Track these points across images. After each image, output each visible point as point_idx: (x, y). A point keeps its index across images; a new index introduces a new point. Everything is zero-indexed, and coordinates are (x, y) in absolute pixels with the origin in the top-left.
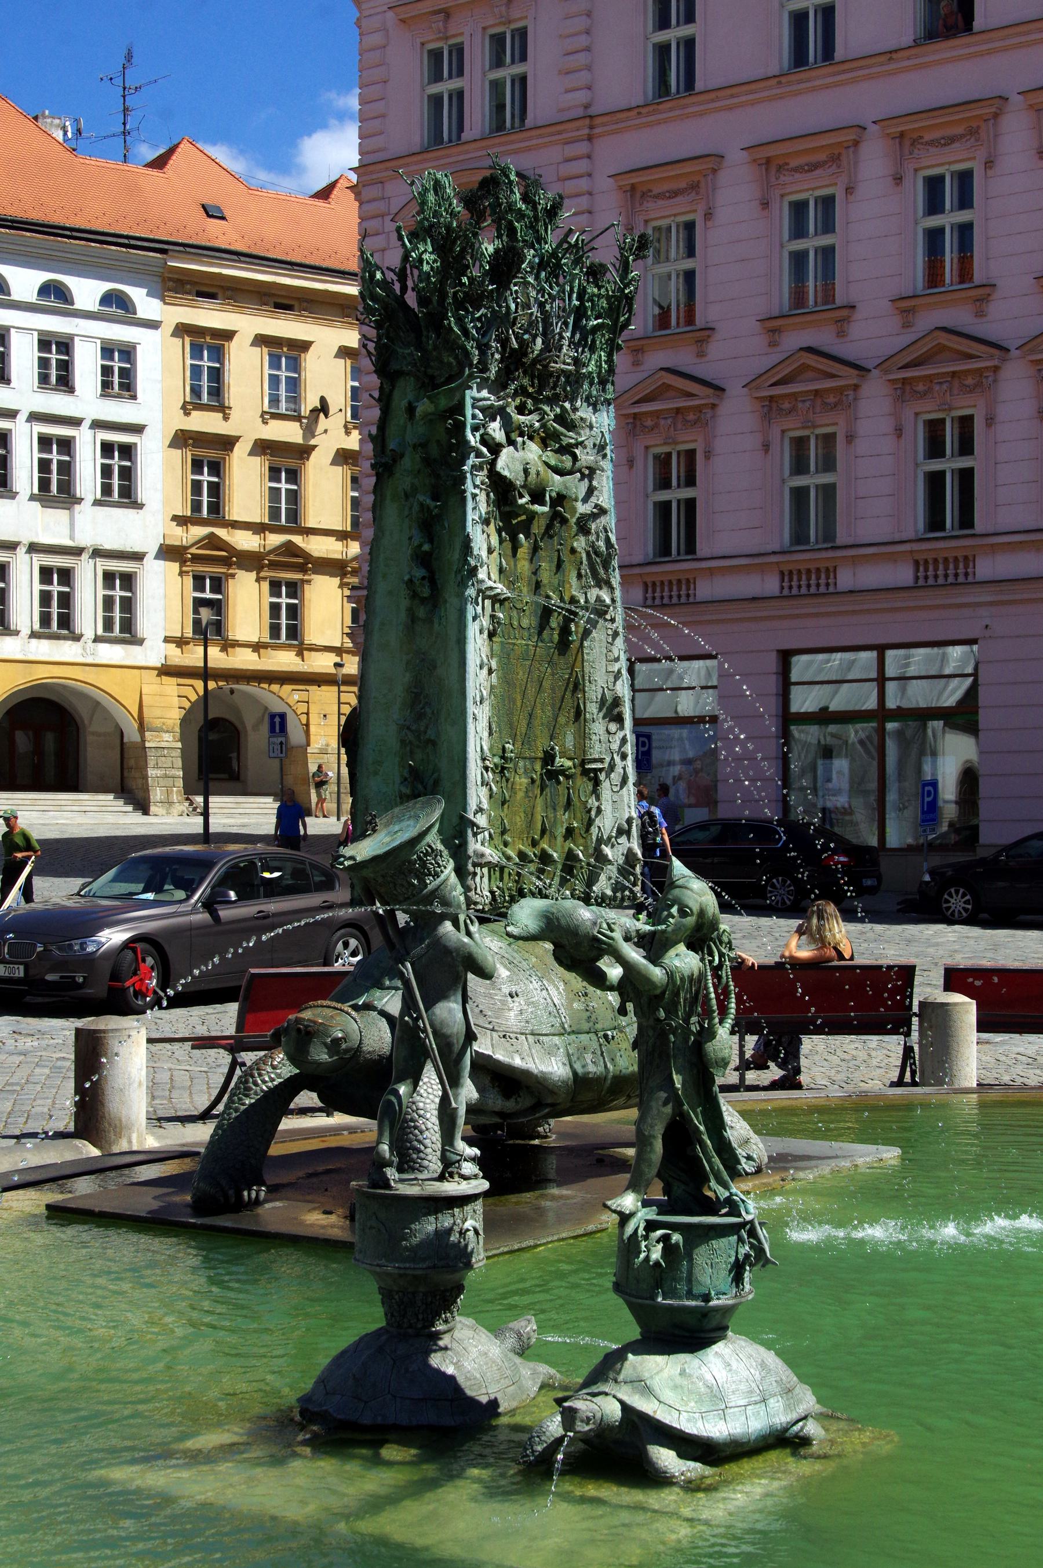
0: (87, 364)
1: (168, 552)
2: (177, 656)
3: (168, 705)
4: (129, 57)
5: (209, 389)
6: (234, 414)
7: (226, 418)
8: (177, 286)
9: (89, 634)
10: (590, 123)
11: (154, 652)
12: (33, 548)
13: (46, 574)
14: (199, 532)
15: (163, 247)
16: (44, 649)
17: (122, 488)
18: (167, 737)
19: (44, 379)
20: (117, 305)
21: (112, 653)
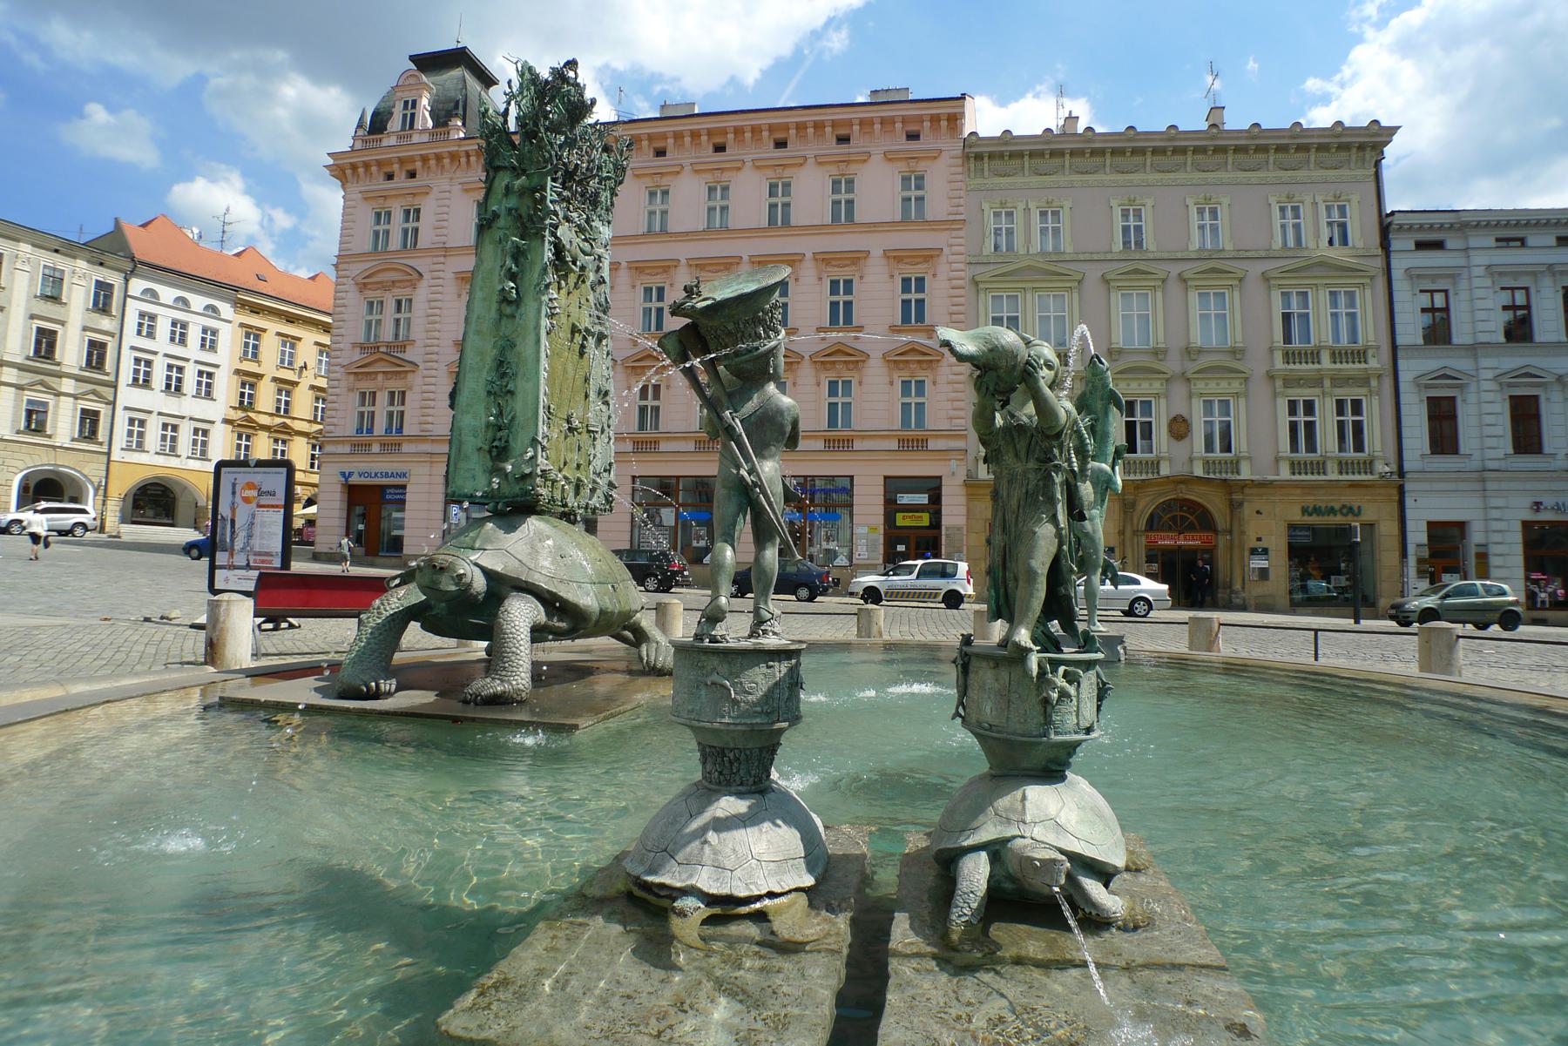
5: (252, 351)
8: (241, 305)
9: (184, 455)
10: (446, 251)
12: (160, 414)
15: (236, 289)
16: (161, 460)
17: (206, 391)
19: (172, 339)
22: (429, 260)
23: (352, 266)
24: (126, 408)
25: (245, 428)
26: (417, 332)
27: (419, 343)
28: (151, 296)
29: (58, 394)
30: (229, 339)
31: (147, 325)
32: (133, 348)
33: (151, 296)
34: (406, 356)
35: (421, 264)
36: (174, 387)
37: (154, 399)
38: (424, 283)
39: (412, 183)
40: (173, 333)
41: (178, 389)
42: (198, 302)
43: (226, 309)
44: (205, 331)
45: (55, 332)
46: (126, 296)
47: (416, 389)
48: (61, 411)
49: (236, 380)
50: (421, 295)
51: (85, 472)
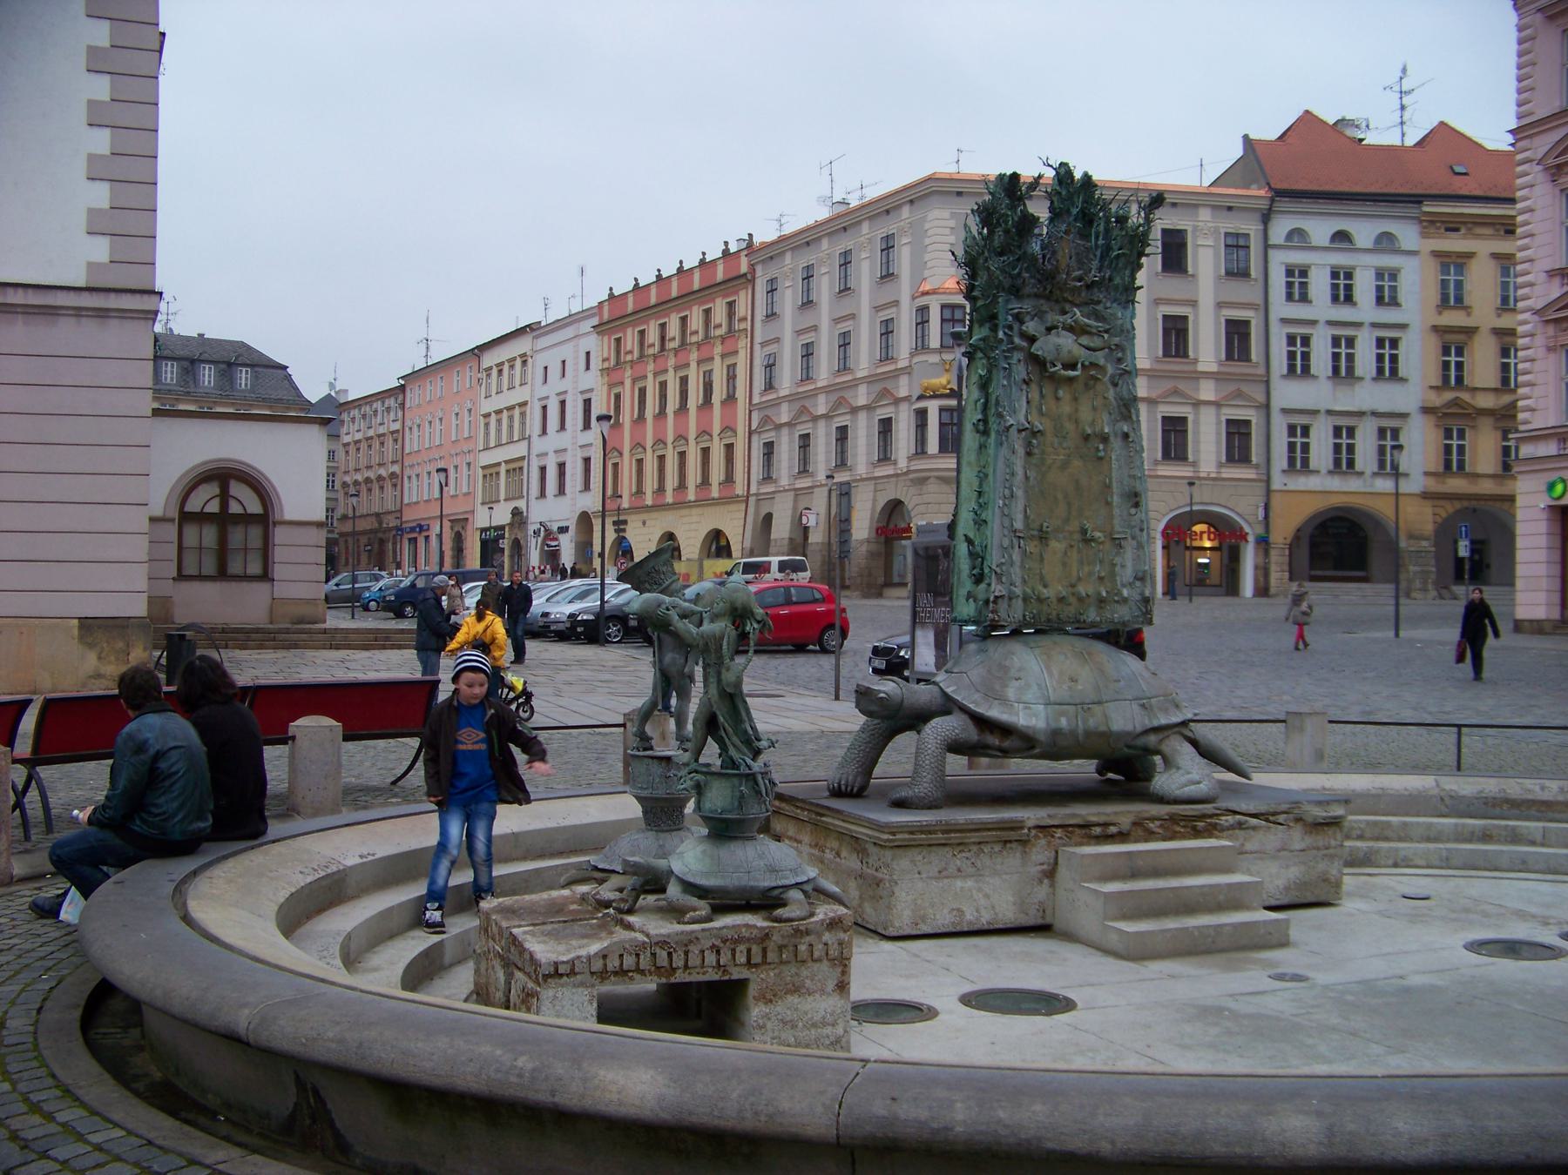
0: (1364, 287)
1: (1426, 410)
2: (1432, 485)
3: (1420, 519)
4: (1404, 70)
5: (1451, 297)
6: (1476, 312)
7: (1469, 314)
8: (1431, 225)
11: (1414, 484)
12: (1329, 412)
13: (1337, 431)
14: (1449, 396)
15: (1417, 199)
16: (1335, 483)
17: (1388, 369)
18: (1424, 543)
19: (1335, 299)
20: (1386, 242)
23: (1537, 141)
24: (1285, 411)
25: (1453, 419)
28: (1297, 237)
29: (1197, 404)
30: (1417, 284)
31: (1298, 286)
32: (1284, 321)
33: (1297, 237)
36: (1343, 371)
40: (1335, 287)
41: (1350, 369)
42: (1364, 231)
43: (1407, 234)
44: (1379, 275)
45: (1185, 318)
46: (1267, 246)
48: (1203, 428)
49: (1433, 343)
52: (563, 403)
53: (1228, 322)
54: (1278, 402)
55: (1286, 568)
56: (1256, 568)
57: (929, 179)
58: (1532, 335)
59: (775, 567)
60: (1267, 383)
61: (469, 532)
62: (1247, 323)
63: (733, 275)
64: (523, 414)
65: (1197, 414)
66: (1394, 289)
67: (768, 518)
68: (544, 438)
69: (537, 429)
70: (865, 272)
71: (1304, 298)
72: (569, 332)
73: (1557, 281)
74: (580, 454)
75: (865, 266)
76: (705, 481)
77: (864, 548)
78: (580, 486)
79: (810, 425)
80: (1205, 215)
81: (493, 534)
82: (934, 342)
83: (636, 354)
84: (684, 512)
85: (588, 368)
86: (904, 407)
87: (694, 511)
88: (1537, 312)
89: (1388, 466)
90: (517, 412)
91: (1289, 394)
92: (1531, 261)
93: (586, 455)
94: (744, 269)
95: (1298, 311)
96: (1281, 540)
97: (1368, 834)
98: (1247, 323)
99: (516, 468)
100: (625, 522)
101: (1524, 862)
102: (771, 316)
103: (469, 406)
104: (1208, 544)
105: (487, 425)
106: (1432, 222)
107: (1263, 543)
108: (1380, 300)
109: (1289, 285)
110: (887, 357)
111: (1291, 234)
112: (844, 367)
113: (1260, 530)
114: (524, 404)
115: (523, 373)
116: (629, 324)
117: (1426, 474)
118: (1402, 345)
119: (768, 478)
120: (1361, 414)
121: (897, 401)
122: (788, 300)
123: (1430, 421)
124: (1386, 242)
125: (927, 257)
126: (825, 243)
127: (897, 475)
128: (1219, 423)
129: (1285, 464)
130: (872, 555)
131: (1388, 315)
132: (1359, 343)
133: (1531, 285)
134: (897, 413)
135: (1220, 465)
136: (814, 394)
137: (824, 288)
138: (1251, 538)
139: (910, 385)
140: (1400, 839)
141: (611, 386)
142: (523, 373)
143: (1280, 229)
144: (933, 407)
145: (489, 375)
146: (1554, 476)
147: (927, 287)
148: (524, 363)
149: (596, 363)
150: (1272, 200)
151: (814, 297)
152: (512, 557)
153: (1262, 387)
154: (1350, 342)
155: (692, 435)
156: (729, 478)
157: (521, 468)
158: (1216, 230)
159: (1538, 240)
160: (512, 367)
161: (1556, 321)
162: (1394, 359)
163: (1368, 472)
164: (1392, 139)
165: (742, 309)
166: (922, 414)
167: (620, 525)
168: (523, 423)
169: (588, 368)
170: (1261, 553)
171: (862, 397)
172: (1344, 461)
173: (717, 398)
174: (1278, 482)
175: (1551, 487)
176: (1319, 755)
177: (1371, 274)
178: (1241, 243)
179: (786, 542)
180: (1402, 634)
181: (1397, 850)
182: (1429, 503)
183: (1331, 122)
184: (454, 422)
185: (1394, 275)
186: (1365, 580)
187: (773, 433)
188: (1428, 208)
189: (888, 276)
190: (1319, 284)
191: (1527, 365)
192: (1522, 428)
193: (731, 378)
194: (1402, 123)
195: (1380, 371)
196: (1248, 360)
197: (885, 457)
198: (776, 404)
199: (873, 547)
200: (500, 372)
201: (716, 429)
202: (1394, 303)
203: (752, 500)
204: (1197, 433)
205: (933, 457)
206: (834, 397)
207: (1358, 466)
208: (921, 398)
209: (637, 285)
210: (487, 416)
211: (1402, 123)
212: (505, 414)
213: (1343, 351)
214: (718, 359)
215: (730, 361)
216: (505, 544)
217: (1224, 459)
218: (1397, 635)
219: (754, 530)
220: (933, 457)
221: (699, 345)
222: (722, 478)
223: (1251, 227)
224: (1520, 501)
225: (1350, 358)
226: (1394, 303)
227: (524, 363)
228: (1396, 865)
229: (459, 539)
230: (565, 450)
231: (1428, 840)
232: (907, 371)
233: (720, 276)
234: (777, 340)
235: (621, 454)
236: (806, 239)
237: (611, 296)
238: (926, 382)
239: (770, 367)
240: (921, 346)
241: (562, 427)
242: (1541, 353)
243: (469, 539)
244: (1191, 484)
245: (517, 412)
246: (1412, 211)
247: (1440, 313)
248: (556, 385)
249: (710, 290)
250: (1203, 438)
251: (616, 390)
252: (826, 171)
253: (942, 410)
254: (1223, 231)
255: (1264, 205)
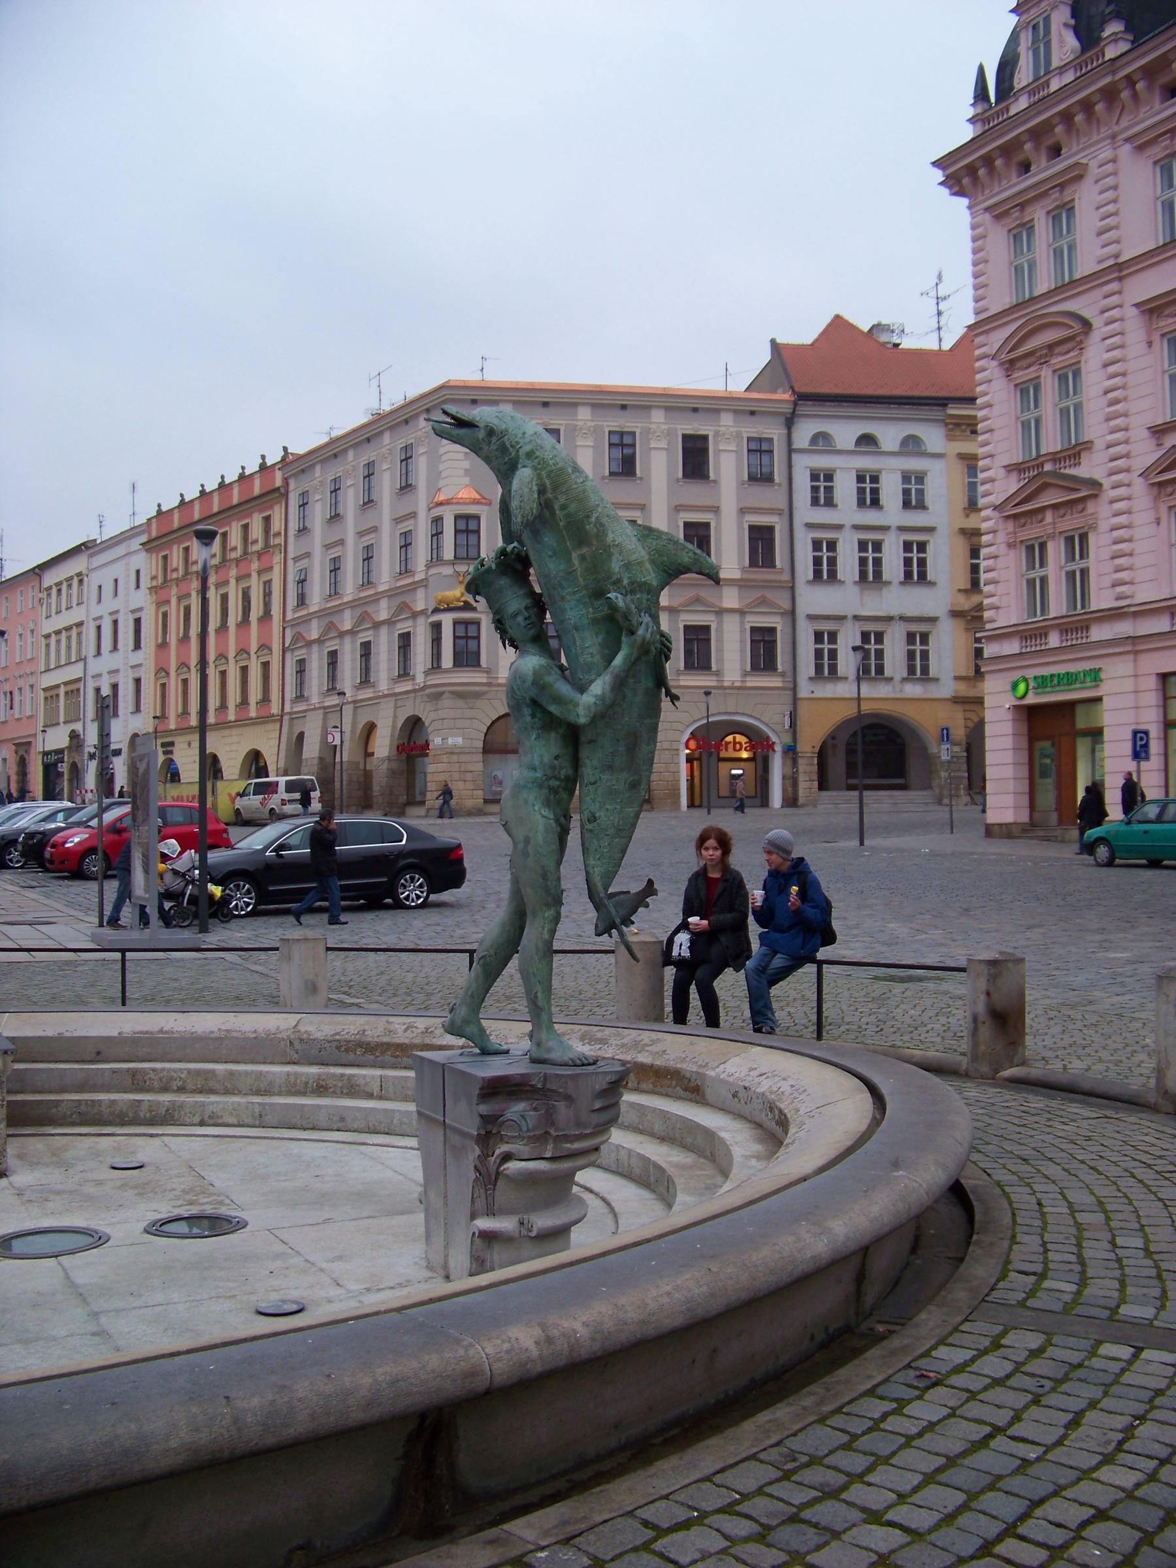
0: (891, 490)
1: (955, 614)
4: (940, 277)
10: (1120, 270)
12: (856, 618)
15: (942, 402)
17: (916, 574)
19: (861, 503)
20: (911, 445)
21: (913, 690)
22: (1097, 294)
24: (811, 617)
26: (1094, 428)
27: (1099, 444)
28: (821, 440)
29: (720, 612)
31: (823, 488)
32: (809, 526)
33: (821, 440)
34: (1083, 471)
35: (1085, 305)
36: (871, 575)
37: (841, 599)
38: (1095, 336)
39: (1060, 165)
40: (861, 491)
41: (878, 574)
42: (890, 434)
43: (933, 437)
44: (906, 478)
45: (707, 525)
46: (790, 451)
47: (1103, 526)
48: (726, 636)
50: (1094, 355)
51: (766, 720)
52: (115, 622)
53: (752, 528)
54: (803, 609)
55: (815, 777)
56: (784, 778)
57: (442, 387)
58: (995, 532)
59: (282, 787)
60: (793, 589)
61: (32, 755)
62: (770, 529)
63: (264, 492)
64: (79, 634)
65: (720, 623)
66: (920, 492)
67: (301, 736)
68: (99, 658)
69: (92, 650)
70: (386, 483)
71: (830, 503)
72: (120, 550)
73: (1014, 476)
74: (131, 675)
75: (387, 477)
76: (244, 702)
77: (385, 766)
78: (131, 707)
79: (337, 641)
80: (727, 420)
81: (54, 757)
82: (448, 553)
83: (181, 572)
84: (226, 732)
85: (138, 587)
86: (421, 621)
87: (234, 731)
88: (996, 508)
89: (918, 667)
90: (74, 632)
91: (815, 600)
92: (991, 456)
93: (137, 676)
94: (278, 482)
95: (823, 516)
96: (809, 749)
97: (190, 1086)
98: (770, 529)
99: (73, 689)
100: (172, 744)
101: (342, 1119)
102: (303, 530)
103: (32, 626)
104: (745, 755)
105: (48, 646)
106: (957, 425)
107: (791, 751)
108: (906, 504)
109: (815, 489)
110: (406, 570)
111: (815, 439)
112: (368, 583)
113: (788, 739)
114: (80, 624)
115: (80, 592)
116: (172, 542)
117: (956, 678)
118: (930, 548)
119: (300, 697)
120: (890, 619)
121: (415, 615)
122: (318, 513)
123: (960, 624)
124: (911, 445)
125: (442, 467)
126: (351, 454)
127: (414, 691)
128: (743, 631)
129: (812, 673)
130: (393, 773)
131: (915, 519)
132: (885, 548)
133: (993, 480)
134: (415, 627)
135: (745, 674)
136: (339, 610)
137: (351, 499)
138: (778, 748)
139: (426, 598)
140: (227, 1092)
141: (159, 605)
142: (80, 592)
143: (804, 432)
144: (447, 620)
145: (49, 595)
146: (1017, 675)
147: (442, 497)
148: (81, 582)
149: (145, 582)
150: (795, 404)
151: (341, 510)
152: (70, 781)
153: (786, 595)
154: (878, 546)
155: (231, 654)
156: (266, 699)
157: (78, 690)
158: (738, 435)
159: (997, 435)
160: (70, 586)
161: (1015, 517)
162: (922, 563)
163: (898, 678)
164: (931, 344)
165: (277, 525)
166: (437, 627)
167: (168, 747)
168: (79, 643)
169: (138, 587)
170: (789, 762)
171: (383, 612)
172: (871, 667)
173: (254, 616)
174: (803, 693)
175: (1015, 686)
176: (312, 988)
177: (898, 478)
178: (765, 447)
179: (316, 762)
180: (866, 843)
181: (203, 1105)
182: (959, 708)
183: (865, 328)
184: (18, 643)
185: (920, 479)
186: (904, 787)
187: (304, 651)
188: (952, 410)
189: (407, 487)
190: (845, 488)
191: (991, 562)
192: (988, 626)
193: (267, 595)
194: (939, 329)
195: (908, 575)
196: (773, 566)
197: (405, 673)
198: (306, 620)
199: (394, 765)
200: (59, 591)
201: (254, 647)
202: (921, 506)
203: (286, 718)
204: (720, 641)
205: (447, 671)
206: (358, 612)
207: (888, 672)
208: (436, 611)
209: (183, 500)
210: (47, 636)
211: (939, 329)
212: (64, 635)
213: (870, 555)
214: (254, 575)
215: (265, 578)
216: (64, 768)
217: (748, 668)
218: (862, 843)
219: (287, 750)
220: (447, 671)
221: (237, 561)
222: (260, 697)
223: (774, 431)
224: (988, 702)
225: (878, 562)
226: (921, 506)
227: (81, 582)
228: (202, 1124)
229: (23, 763)
230: (117, 671)
231: (258, 1093)
232: (424, 584)
233: (257, 491)
234: (308, 555)
235: (168, 674)
236: (333, 451)
237: (160, 513)
238: (441, 594)
239: (301, 582)
240: (436, 559)
241: (115, 648)
242: (1003, 549)
243: (32, 763)
244: (707, 694)
245: (74, 632)
246: (937, 413)
247: (967, 516)
248: (109, 604)
249: (249, 504)
250: (726, 647)
251: (163, 609)
252: (375, 383)
253: (456, 623)
254: (745, 436)
255: (787, 408)
